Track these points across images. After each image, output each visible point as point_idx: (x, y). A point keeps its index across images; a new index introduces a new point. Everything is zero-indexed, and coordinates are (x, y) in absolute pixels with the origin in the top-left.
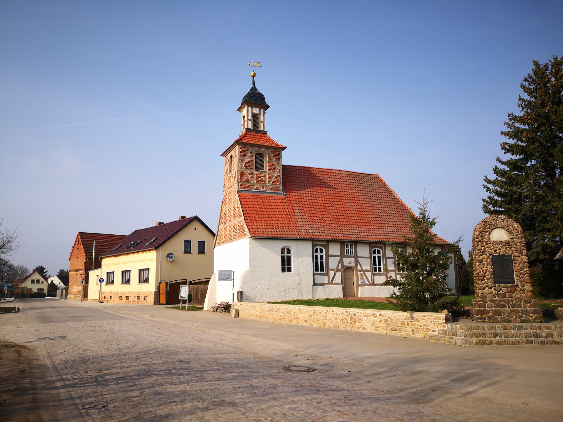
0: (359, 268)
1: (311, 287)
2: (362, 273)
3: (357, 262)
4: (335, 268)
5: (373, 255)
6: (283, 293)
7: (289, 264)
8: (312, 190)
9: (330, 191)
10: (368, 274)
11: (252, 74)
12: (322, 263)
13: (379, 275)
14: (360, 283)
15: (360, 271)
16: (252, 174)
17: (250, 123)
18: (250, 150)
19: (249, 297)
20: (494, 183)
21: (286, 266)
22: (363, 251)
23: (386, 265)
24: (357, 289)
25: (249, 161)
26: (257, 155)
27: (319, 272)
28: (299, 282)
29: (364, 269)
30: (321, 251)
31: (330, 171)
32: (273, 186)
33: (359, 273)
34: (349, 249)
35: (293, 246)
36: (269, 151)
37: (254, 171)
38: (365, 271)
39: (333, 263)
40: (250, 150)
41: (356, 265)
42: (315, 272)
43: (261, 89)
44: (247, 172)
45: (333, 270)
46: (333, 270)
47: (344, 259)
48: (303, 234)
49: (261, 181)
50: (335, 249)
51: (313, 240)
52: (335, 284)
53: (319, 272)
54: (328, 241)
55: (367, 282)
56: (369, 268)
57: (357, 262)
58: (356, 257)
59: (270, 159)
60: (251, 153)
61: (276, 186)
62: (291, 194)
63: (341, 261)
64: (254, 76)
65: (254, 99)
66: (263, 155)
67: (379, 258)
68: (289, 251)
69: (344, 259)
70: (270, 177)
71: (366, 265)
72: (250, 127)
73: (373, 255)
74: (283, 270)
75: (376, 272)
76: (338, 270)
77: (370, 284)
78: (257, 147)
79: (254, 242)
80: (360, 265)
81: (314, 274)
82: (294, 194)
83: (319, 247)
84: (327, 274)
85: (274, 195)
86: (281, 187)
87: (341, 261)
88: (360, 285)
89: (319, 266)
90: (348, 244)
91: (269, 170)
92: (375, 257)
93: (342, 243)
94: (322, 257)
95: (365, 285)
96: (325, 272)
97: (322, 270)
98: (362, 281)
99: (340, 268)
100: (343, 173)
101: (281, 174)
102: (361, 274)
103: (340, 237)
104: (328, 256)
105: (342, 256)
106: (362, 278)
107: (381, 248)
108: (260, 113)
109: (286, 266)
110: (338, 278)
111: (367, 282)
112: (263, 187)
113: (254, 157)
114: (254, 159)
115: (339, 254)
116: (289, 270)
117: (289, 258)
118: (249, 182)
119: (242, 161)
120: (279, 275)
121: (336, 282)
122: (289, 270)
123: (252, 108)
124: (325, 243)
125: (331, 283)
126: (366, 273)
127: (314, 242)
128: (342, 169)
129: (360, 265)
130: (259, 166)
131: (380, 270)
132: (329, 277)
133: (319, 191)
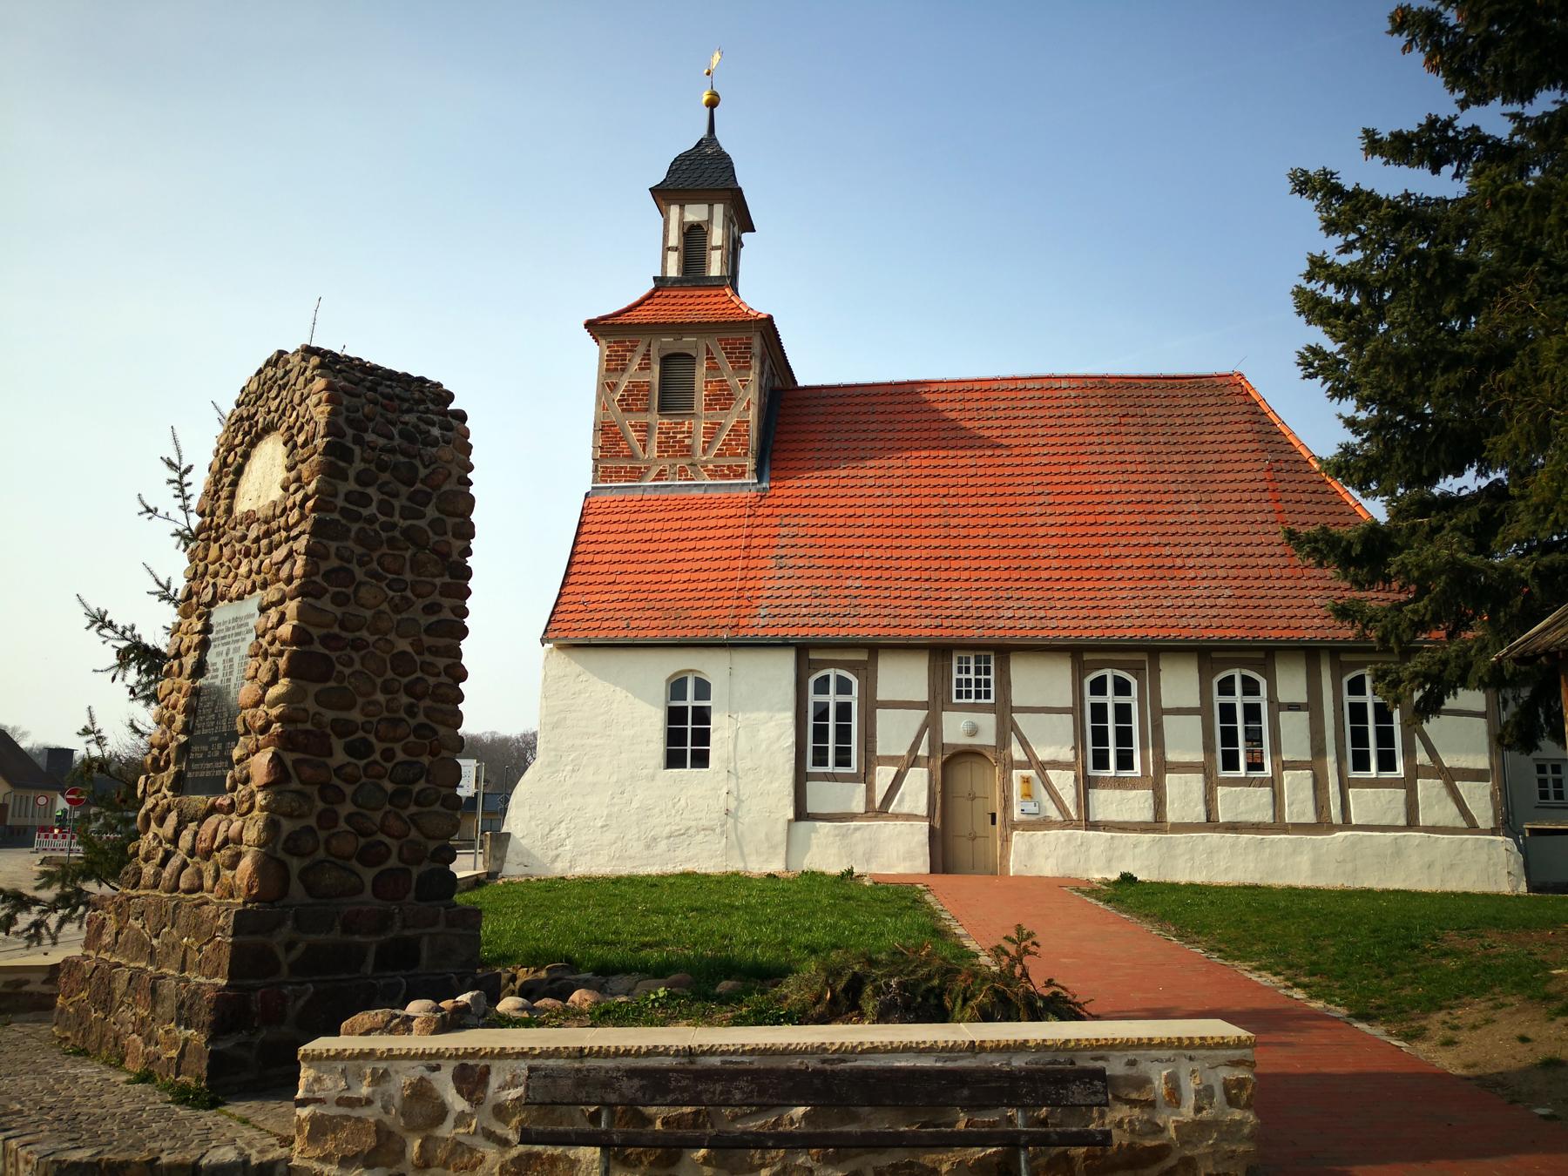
0: (1017, 753)
1: (781, 827)
2: (1031, 773)
3: (1006, 729)
4: (904, 752)
5: (1090, 699)
6: (662, 845)
7: (703, 737)
8: (887, 463)
9: (967, 458)
10: (1064, 782)
11: (706, 97)
12: (844, 734)
13: (1119, 784)
14: (1017, 815)
15: (1021, 765)
16: (646, 429)
17: (673, 257)
18: (641, 349)
19: (529, 854)
20: (1343, 279)
21: (687, 739)
22: (1042, 684)
23: (1158, 741)
24: (1006, 840)
25: (636, 385)
26: (666, 360)
27: (1112, 770)
28: (732, 805)
29: (1043, 754)
30: (844, 687)
31: (1004, 385)
32: (721, 461)
33: (1017, 774)
34: (972, 676)
35: (712, 666)
36: (713, 342)
37: (654, 418)
38: (1043, 767)
39: (896, 732)
40: (641, 349)
41: (1003, 742)
42: (1092, 772)
43: (727, 141)
44: (628, 421)
45: (890, 760)
46: (890, 760)
47: (947, 717)
48: (758, 626)
49: (676, 447)
50: (903, 679)
51: (802, 649)
52: (896, 817)
53: (1112, 770)
54: (875, 648)
55: (1053, 813)
56: (1067, 754)
57: (1006, 729)
58: (1005, 711)
59: (713, 368)
60: (647, 356)
61: (733, 461)
62: (789, 483)
63: (932, 725)
64: (713, 104)
65: (702, 179)
66: (688, 358)
67: (1123, 712)
68: (703, 689)
69: (947, 717)
70: (712, 432)
71: (1053, 740)
72: (673, 272)
73: (1218, 699)
74: (674, 760)
75: (1102, 773)
76: (914, 761)
77: (1068, 823)
78: (667, 335)
79: (562, 658)
80: (1024, 744)
81: (801, 779)
82: (798, 487)
83: (832, 673)
84: (866, 776)
85: (721, 494)
86: (750, 463)
87: (932, 725)
88: (1015, 826)
89: (827, 743)
90: (970, 660)
91: (709, 407)
92: (1228, 712)
93: (939, 652)
94: (844, 711)
95: (1045, 824)
96: (854, 768)
97: (843, 760)
98: (1030, 807)
99: (923, 751)
100: (1064, 384)
101: (752, 416)
102: (1026, 781)
103: (923, 630)
104: (871, 705)
105: (936, 704)
106: (1028, 795)
107: (1137, 670)
108: (710, 221)
109: (687, 739)
110: (916, 791)
111: (1053, 813)
112: (682, 470)
113: (656, 368)
114: (654, 376)
115: (923, 696)
116: (701, 760)
117: (702, 715)
118: (632, 457)
119: (613, 387)
120: (653, 778)
121: (905, 809)
122: (701, 760)
123: (682, 207)
124: (862, 656)
125: (879, 811)
126: (1052, 774)
127: (807, 653)
128: (1058, 372)
129: (1024, 744)
130: (673, 398)
131: (1125, 762)
132: (870, 790)
133: (916, 463)
